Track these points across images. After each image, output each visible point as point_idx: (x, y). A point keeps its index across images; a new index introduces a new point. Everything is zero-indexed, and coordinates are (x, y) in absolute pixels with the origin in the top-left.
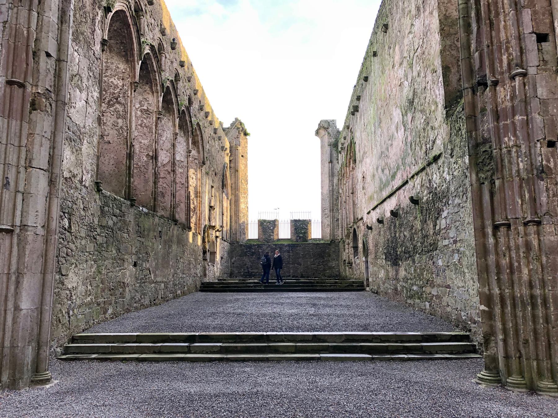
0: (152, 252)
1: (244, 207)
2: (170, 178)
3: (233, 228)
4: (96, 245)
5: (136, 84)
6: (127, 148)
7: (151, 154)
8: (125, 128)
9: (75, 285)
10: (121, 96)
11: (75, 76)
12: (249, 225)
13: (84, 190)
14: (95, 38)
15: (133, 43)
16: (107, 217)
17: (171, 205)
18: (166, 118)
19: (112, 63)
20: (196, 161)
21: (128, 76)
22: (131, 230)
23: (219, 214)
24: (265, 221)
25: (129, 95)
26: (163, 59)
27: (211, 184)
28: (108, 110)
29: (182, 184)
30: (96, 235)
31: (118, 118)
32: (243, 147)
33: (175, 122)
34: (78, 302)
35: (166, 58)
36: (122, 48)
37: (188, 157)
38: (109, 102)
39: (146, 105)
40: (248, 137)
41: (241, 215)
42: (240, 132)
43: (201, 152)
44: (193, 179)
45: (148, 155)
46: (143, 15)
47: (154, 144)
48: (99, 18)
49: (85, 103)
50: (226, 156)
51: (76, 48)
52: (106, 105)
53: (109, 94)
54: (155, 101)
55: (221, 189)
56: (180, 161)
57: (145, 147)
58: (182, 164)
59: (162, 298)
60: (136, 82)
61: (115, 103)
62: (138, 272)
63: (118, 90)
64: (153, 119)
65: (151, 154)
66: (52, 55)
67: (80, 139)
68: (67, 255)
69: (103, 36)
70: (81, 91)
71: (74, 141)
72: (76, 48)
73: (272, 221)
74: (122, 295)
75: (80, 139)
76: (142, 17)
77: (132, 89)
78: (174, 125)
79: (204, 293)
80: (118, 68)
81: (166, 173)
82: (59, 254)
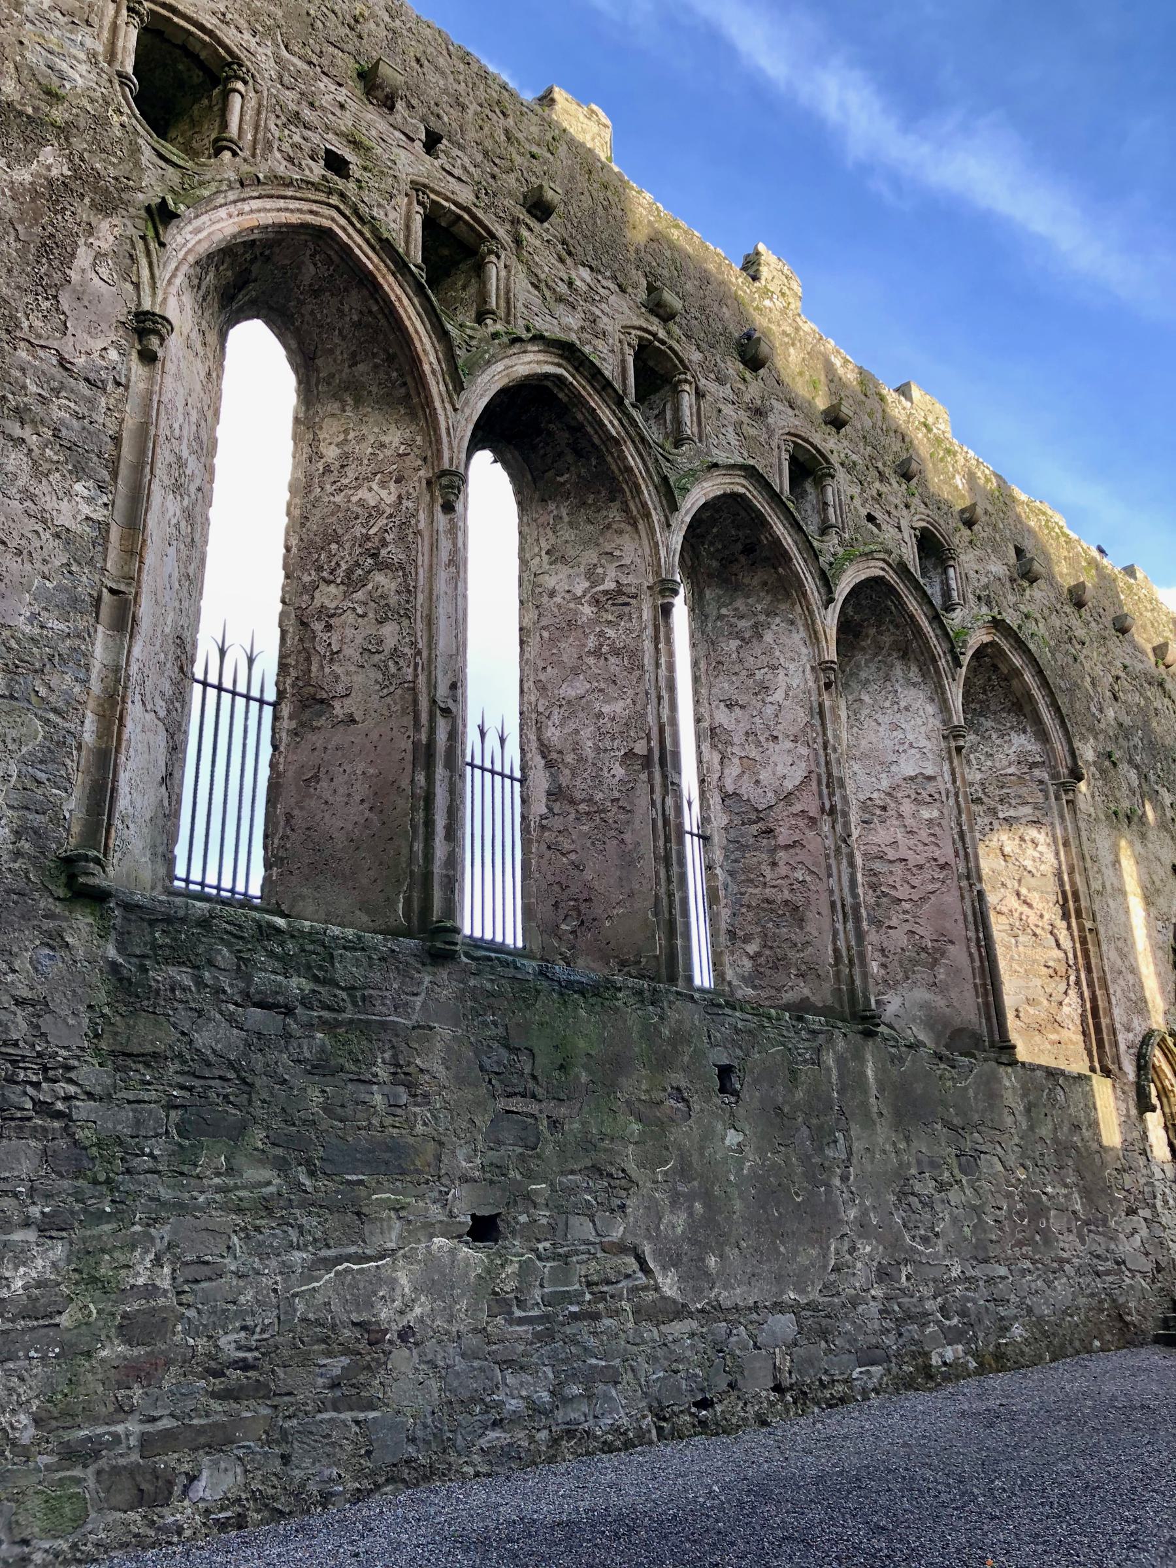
5: (444, 481)
7: (640, 748)
8: (406, 650)
10: (389, 538)
14: (65, 305)
16: (183, 1018)
17: (836, 951)
18: (778, 620)
20: (1037, 773)
21: (420, 462)
22: (440, 1071)
26: (687, 400)
29: (943, 867)
30: (67, 1098)
33: (813, 622)
35: (700, 394)
36: (395, 374)
38: (349, 572)
39: (612, 572)
43: (1056, 735)
45: (630, 754)
46: (490, 252)
52: (342, 587)
53: (347, 546)
56: (920, 778)
57: (616, 728)
58: (931, 788)
59: (778, 1388)
61: (369, 572)
63: (382, 522)
65: (640, 748)
69: (139, 304)
76: (493, 258)
78: (814, 637)
80: (383, 445)
81: (802, 823)
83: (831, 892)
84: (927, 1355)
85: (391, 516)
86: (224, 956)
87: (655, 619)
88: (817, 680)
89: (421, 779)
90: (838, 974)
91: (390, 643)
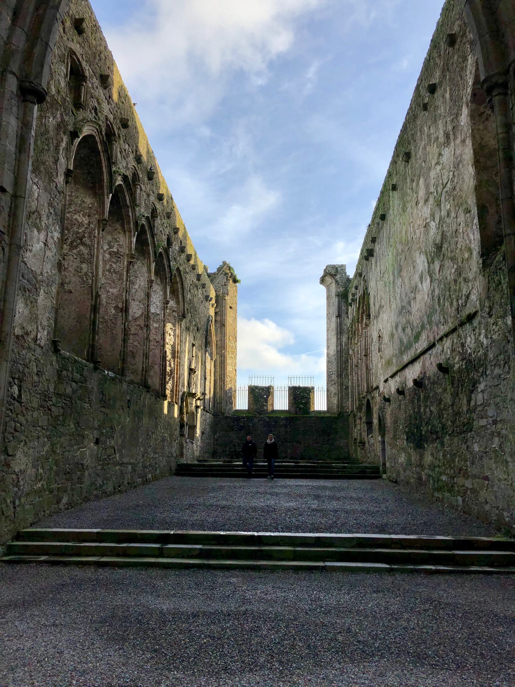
0: (118, 426)
1: (231, 370)
2: (142, 334)
3: (218, 396)
4: (50, 417)
5: (104, 222)
6: (92, 299)
7: (120, 305)
8: (90, 274)
9: (23, 467)
10: (86, 235)
11: (33, 213)
12: (237, 392)
13: (39, 350)
15: (102, 173)
17: (143, 367)
18: (139, 262)
19: (77, 197)
20: (174, 313)
21: (96, 212)
23: (201, 379)
24: (257, 387)
25: (96, 234)
26: (138, 191)
27: (192, 341)
28: (70, 253)
29: (157, 342)
30: (51, 405)
31: (82, 262)
32: (231, 297)
33: (150, 267)
34: (27, 489)
35: (141, 190)
36: (89, 178)
37: (165, 308)
38: (72, 243)
39: (116, 246)
40: (237, 284)
41: (228, 379)
42: (229, 278)
43: (181, 303)
44: (170, 335)
46: (115, 140)
47: (124, 294)
48: (64, 144)
49: (43, 246)
50: (211, 307)
51: (36, 180)
52: (68, 247)
53: (71, 233)
54: (127, 242)
55: (203, 347)
58: (158, 317)
60: (105, 220)
61: (79, 244)
62: (100, 452)
63: (83, 229)
64: (124, 263)
65: (120, 305)
66: (8, 190)
67: (36, 289)
68: (15, 430)
69: (68, 166)
70: (39, 231)
71: (29, 291)
72: (36, 180)
73: (266, 388)
74: (80, 480)
75: (36, 289)
77: (99, 227)
78: (149, 271)
79: (180, 478)
80: (84, 202)
81: (138, 328)
82: (6, 429)
83: (144, 350)
84: (146, 476)
85: (86, 228)
86: (70, 369)
87: (128, 265)
88: (148, 284)
89: (92, 316)
90: (142, 374)
91: (85, 270)
